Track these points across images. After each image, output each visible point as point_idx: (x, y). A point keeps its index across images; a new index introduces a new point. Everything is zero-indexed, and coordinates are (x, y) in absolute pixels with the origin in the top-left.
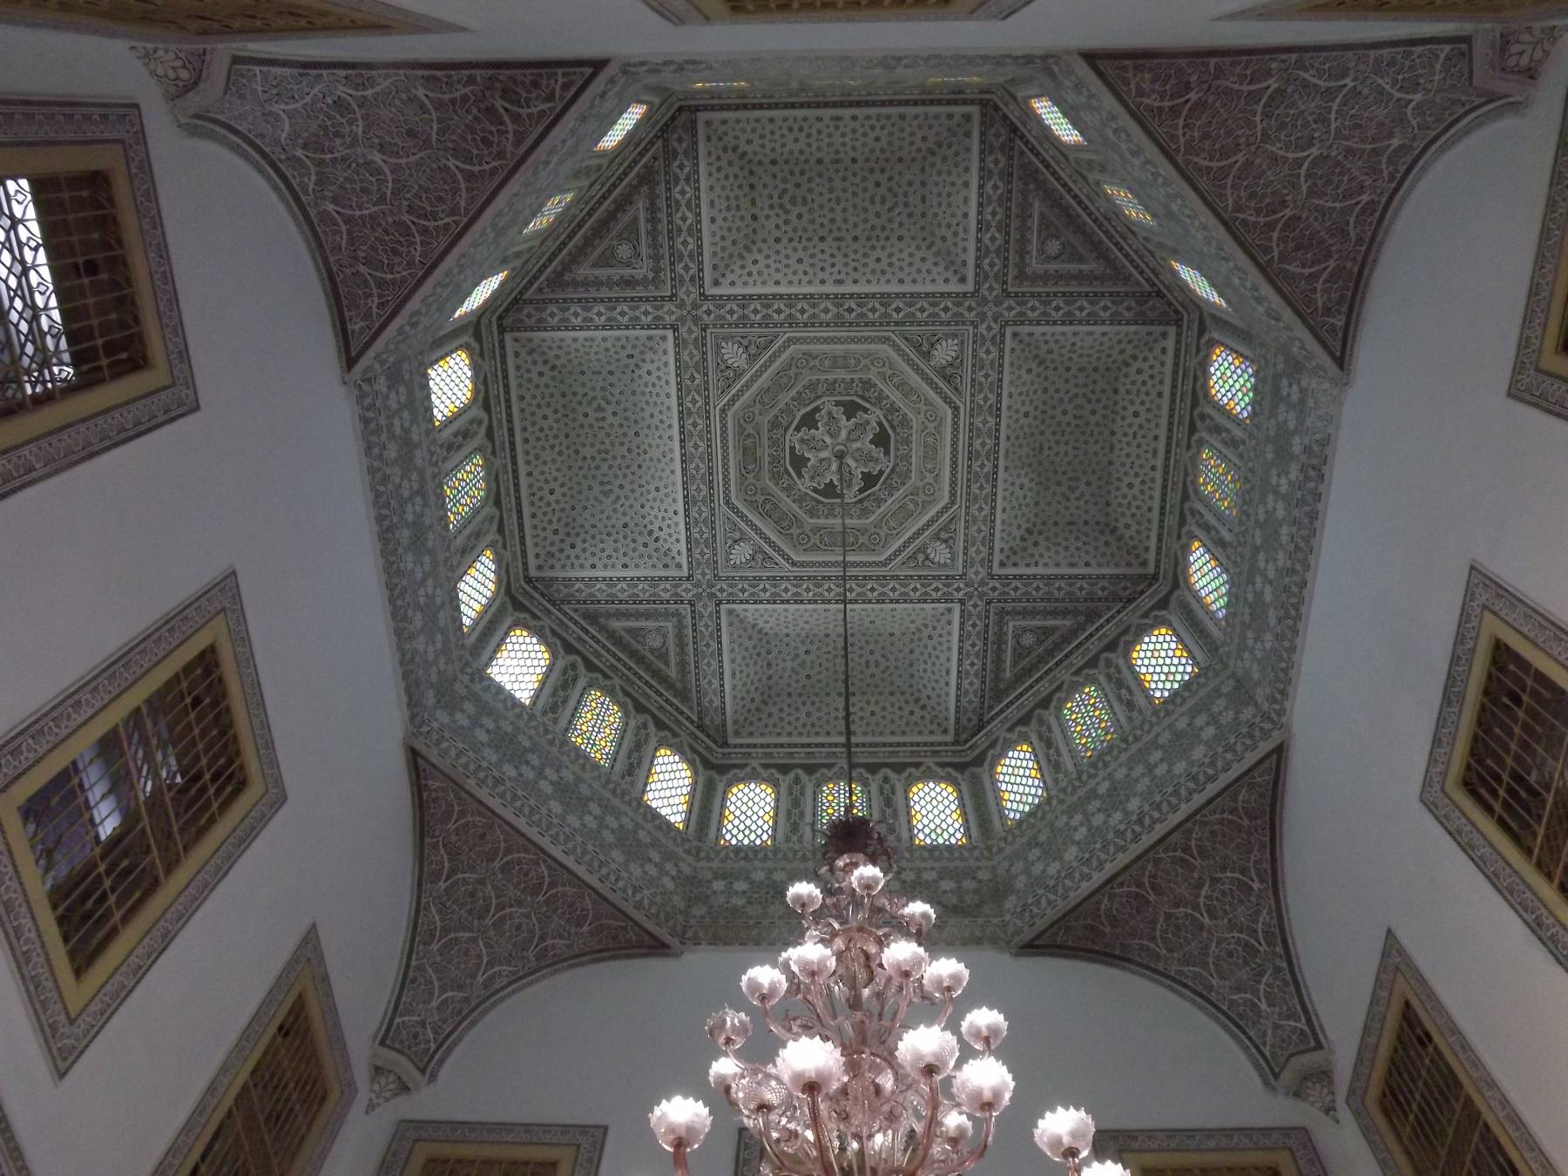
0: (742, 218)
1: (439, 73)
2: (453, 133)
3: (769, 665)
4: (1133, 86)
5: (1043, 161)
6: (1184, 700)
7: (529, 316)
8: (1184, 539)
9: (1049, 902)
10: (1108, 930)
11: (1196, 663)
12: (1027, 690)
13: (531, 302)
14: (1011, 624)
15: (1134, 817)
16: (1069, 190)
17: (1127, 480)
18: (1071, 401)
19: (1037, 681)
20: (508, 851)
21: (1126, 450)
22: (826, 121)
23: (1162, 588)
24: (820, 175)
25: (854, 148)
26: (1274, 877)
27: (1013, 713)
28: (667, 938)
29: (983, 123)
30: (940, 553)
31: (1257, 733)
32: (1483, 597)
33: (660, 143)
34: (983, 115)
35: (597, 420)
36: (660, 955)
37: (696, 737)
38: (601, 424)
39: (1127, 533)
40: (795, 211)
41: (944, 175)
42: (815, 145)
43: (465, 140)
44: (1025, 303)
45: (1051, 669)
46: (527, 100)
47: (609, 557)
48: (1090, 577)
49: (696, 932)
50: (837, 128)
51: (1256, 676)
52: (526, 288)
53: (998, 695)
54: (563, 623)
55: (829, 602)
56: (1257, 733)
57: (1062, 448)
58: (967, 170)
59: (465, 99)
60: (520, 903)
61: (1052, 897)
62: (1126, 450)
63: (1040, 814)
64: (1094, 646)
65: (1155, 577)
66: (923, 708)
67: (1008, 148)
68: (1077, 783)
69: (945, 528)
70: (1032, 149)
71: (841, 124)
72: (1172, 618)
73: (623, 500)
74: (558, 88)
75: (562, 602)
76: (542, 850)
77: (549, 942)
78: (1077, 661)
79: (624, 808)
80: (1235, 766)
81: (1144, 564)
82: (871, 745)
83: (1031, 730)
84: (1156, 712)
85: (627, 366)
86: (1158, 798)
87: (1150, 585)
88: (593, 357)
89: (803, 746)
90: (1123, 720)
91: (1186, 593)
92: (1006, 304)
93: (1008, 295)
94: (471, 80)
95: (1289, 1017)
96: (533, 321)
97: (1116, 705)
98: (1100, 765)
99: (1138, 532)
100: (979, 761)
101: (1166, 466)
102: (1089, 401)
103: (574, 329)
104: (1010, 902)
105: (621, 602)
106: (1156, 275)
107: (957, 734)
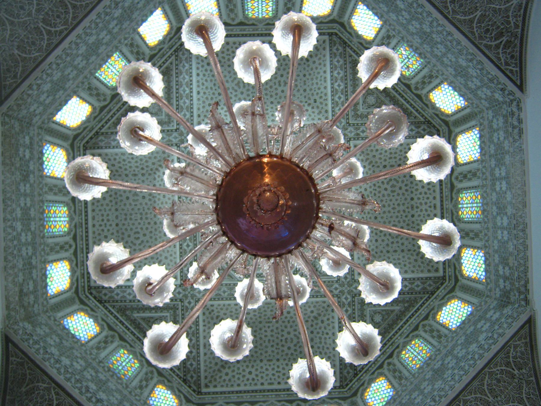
0: (385, 160)
1: (522, 11)
2: (493, 16)
4: (518, 343)
5: (418, 309)
7: (337, 49)
9: (38, 350)
10: (24, 389)
12: (126, 327)
13: (345, 51)
14: (168, 314)
16: (405, 323)
17: (253, 370)
18: (295, 335)
19: (132, 332)
21: (270, 368)
22: (434, 202)
24: (406, 199)
25: (419, 216)
29: (435, 278)
33: (422, 120)
34: (439, 278)
35: (279, 82)
37: (90, 131)
38: (277, 84)
40: (388, 187)
41: (408, 261)
42: (421, 196)
43: (489, 21)
44: (349, 306)
46: (505, 52)
47: (203, 84)
48: (199, 356)
49: (8, 124)
50: (417, 207)
52: (351, 49)
53: (123, 311)
54: (164, 55)
57: (269, 333)
58: (413, 272)
59: (509, 23)
60: (38, 11)
62: (270, 368)
65: (199, 393)
67: (424, 291)
70: (424, 303)
71: (432, 209)
73: (234, 93)
74: (510, 68)
75: (177, 56)
76: (73, 29)
79: (76, 82)
81: (207, 386)
82: (87, 236)
85: (309, 99)
87: (194, 391)
88: (315, 81)
92: (349, 296)
93: (353, 297)
94: (517, 26)
96: (335, 51)
101: (264, 391)
102: (295, 345)
103: (331, 72)
105: (177, 89)
106: (366, 372)
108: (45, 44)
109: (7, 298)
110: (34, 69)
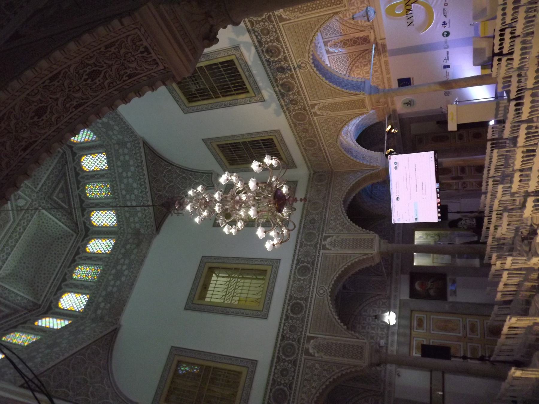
3: (21, 278)
6: (112, 160)
11: (102, 153)
15: (139, 186)
23: (68, 152)
26: (170, 163)
27: (79, 213)
28: (114, 328)
31: (137, 145)
36: (117, 332)
45: (72, 195)
51: (121, 137)
53: (71, 214)
55: (15, 245)
56: (137, 145)
61: (148, 217)
63: (120, 214)
66: (62, 238)
68: (117, 200)
72: (81, 154)
78: (75, 186)
80: (142, 154)
82: (65, 259)
86: (138, 178)
89: (54, 280)
90: (106, 180)
98: (116, 191)
100: (87, 230)
104: (142, 231)
107: (75, 232)
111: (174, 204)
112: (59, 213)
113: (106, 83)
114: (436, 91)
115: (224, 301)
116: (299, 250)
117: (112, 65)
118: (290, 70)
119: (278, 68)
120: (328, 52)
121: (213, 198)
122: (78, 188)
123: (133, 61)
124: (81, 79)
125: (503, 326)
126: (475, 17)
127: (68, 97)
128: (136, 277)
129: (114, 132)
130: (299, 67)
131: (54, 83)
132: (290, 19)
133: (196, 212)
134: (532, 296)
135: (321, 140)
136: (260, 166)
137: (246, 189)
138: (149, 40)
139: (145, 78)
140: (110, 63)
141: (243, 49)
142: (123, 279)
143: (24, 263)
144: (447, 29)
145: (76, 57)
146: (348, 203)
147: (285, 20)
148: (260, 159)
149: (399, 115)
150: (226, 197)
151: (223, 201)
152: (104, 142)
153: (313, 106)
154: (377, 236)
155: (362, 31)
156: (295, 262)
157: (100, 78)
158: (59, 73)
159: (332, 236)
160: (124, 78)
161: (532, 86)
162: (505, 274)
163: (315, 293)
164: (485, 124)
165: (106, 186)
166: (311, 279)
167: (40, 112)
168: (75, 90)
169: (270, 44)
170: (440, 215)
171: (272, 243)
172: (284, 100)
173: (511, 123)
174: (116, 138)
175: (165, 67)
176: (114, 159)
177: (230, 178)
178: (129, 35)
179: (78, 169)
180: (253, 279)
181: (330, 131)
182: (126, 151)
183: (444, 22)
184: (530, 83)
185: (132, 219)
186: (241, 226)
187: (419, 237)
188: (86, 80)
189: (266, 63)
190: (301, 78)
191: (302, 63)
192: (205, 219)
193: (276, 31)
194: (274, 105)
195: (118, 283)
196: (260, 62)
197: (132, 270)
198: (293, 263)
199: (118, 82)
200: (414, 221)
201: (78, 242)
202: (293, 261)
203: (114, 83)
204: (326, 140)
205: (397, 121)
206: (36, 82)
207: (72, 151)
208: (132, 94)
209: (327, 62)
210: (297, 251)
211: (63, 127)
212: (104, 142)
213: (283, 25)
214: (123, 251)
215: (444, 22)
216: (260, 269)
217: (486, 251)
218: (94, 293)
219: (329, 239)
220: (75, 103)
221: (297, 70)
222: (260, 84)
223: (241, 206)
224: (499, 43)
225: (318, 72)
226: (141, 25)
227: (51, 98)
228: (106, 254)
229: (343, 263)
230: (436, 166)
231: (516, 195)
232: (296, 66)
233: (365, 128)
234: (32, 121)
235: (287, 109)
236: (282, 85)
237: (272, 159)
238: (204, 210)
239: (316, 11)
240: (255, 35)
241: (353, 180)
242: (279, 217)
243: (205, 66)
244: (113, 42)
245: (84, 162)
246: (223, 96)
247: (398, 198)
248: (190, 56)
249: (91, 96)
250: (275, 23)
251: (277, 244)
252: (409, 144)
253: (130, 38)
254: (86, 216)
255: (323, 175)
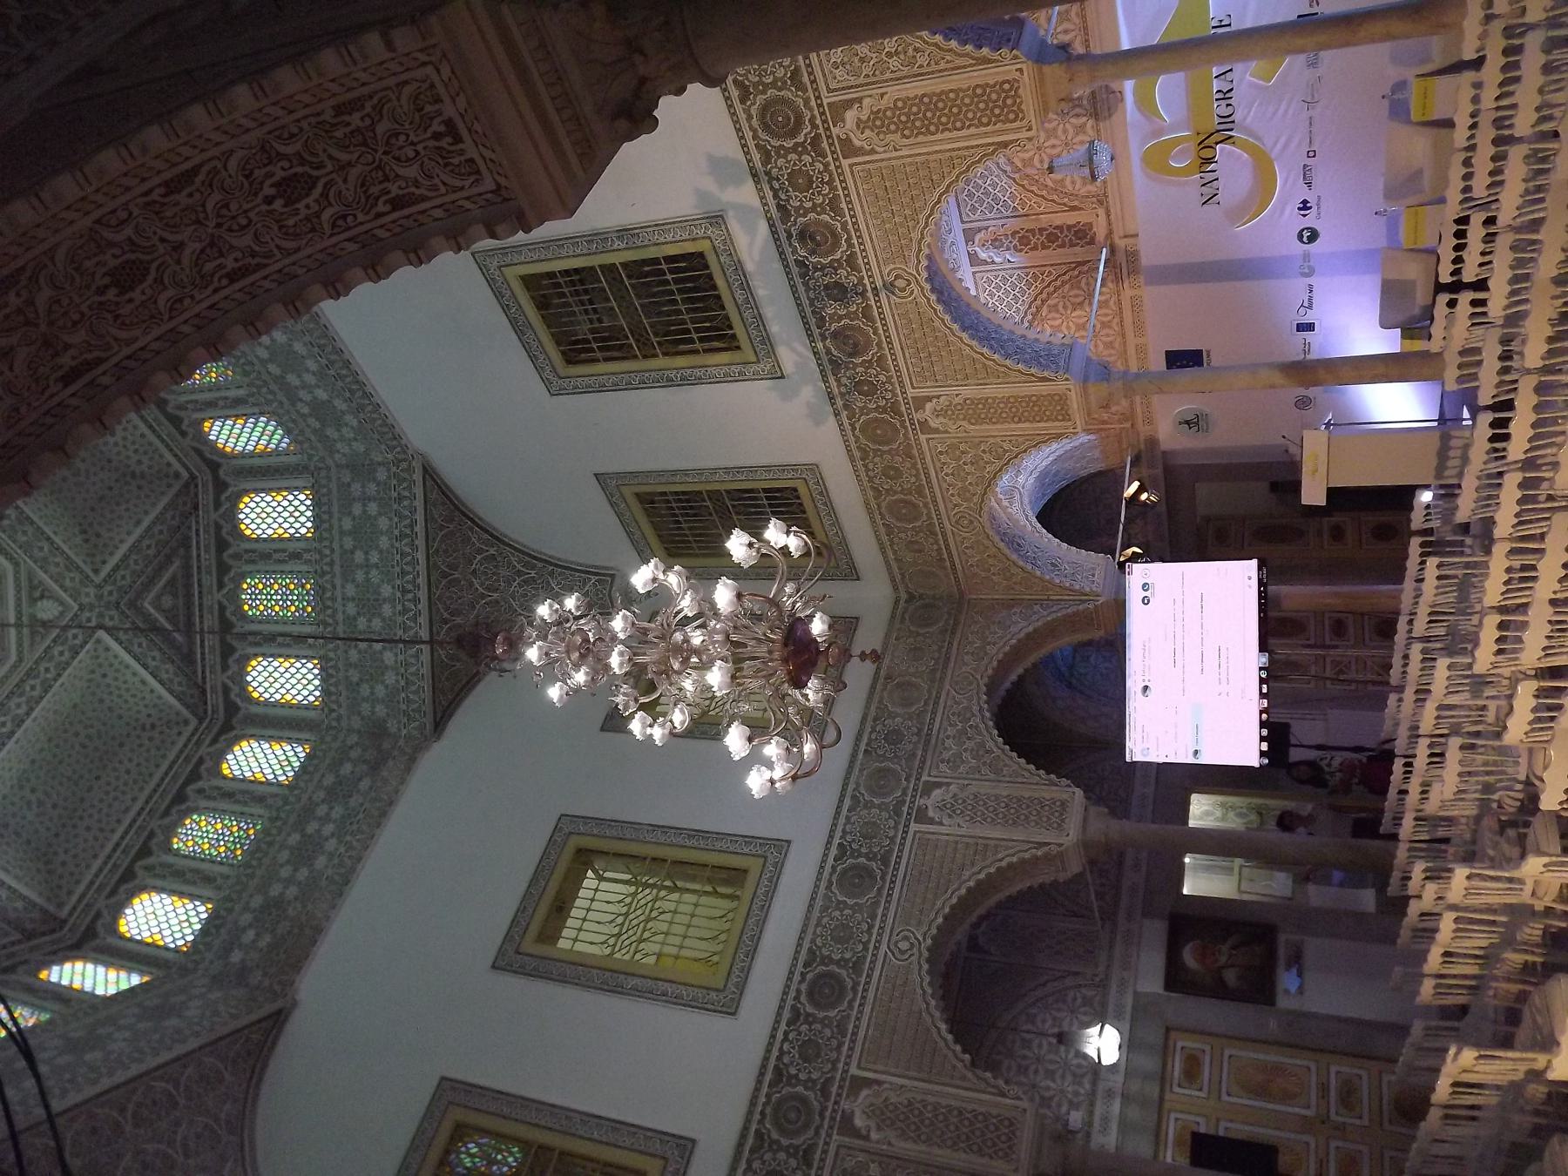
6: (330, 513)
8: (191, 431)
9: (416, 692)
11: (301, 489)
15: (399, 594)
20: (122, 1110)
26: (497, 539)
27: (213, 658)
30: (47, 610)
32: (494, 264)
39: (144, 467)
45: (201, 605)
53: (189, 658)
55: (13, 733)
56: (405, 475)
60: (177, 1124)
64: (209, 558)
65: (193, 477)
69: (32, 588)
72: (242, 486)
77: (223, 1116)
78: (210, 580)
81: (177, 475)
83: (242, 648)
84: (321, 539)
86: (398, 569)
89: (114, 850)
90: (304, 568)
91: (234, 462)
95: (585, 584)
97: (287, 568)
98: (329, 603)
99: (151, 459)
100: (231, 709)
104: (392, 725)
107: (195, 715)
108: (189, 1071)
109: (408, 770)
110: (221, 1039)
111: (492, 641)
112: (156, 654)
113: (326, 215)
114: (1272, 387)
115: (612, 953)
116: (848, 818)
117: (349, 164)
118: (863, 294)
119: (827, 287)
120: (974, 259)
121: (609, 630)
122: (221, 586)
123: (408, 160)
124: (256, 194)
125: (1436, 1071)
126: (1391, 194)
127: (212, 244)
128: (359, 859)
129: (344, 430)
130: (890, 287)
131: (177, 197)
132: (873, 152)
133: (552, 669)
134: (1522, 997)
135: (935, 501)
136: (750, 545)
137: (706, 611)
138: (462, 102)
139: (438, 213)
140: (344, 157)
141: (734, 226)
142: (321, 861)
143: (33, 791)
144: (1311, 221)
145: (248, 130)
146: (1002, 693)
147: (859, 151)
148: (756, 530)
149: (1164, 453)
150: (645, 632)
151: (638, 640)
152: (310, 457)
153: (920, 403)
154: (1079, 792)
155: (1074, 208)
156: (834, 851)
157: (310, 200)
158: (195, 171)
159: (948, 784)
160: (381, 208)
161: (1540, 364)
162: (1447, 924)
163: (884, 947)
164: (1403, 496)
165: (303, 587)
166: (876, 904)
167: (127, 277)
168: (235, 227)
169: (812, 215)
170: (1265, 747)
171: (767, 774)
172: (838, 380)
173: (1479, 478)
174: (346, 450)
175: (498, 185)
176: (335, 509)
177: (661, 576)
178: (406, 82)
179: (226, 533)
180: (706, 893)
181: (964, 480)
182: (372, 488)
183: (1305, 202)
184: (1534, 353)
185: (365, 690)
186: (683, 723)
187: (1203, 810)
188: (269, 200)
189: (795, 270)
190: (895, 320)
191: (897, 277)
192: (577, 690)
193: (831, 180)
194: (810, 392)
195: (303, 873)
196: (777, 266)
197: (348, 838)
198: (825, 855)
199: (361, 217)
200: (1191, 760)
201: (198, 743)
202: (827, 849)
203: (350, 219)
204: (950, 506)
205: (1159, 471)
206: (128, 189)
207: (216, 478)
208: (398, 255)
209: (969, 283)
210: (842, 820)
211: (186, 329)
212: (310, 457)
213: (851, 166)
214: (329, 780)
215: (1305, 202)
216: (725, 867)
217: (1393, 856)
218: (228, 899)
219: (937, 793)
220: (230, 264)
221: (883, 295)
222: (774, 329)
223: (685, 661)
224: (1453, 255)
225: (939, 308)
226: (444, 55)
227: (162, 240)
228: (279, 784)
229: (973, 864)
230: (1260, 604)
231: (1489, 692)
232: (879, 284)
233: (1064, 483)
234: (98, 299)
235: (846, 406)
236: (835, 335)
237: (788, 533)
238: (577, 667)
239: (947, 135)
240: (772, 188)
241: (1021, 627)
242: (796, 702)
243: (625, 265)
244: (359, 99)
245: (247, 510)
246: (665, 354)
247: (1146, 688)
248: (574, 160)
249: (278, 247)
250: (830, 158)
251: (783, 779)
252: (1187, 537)
253: (407, 90)
254: (234, 668)
255: (934, 603)
